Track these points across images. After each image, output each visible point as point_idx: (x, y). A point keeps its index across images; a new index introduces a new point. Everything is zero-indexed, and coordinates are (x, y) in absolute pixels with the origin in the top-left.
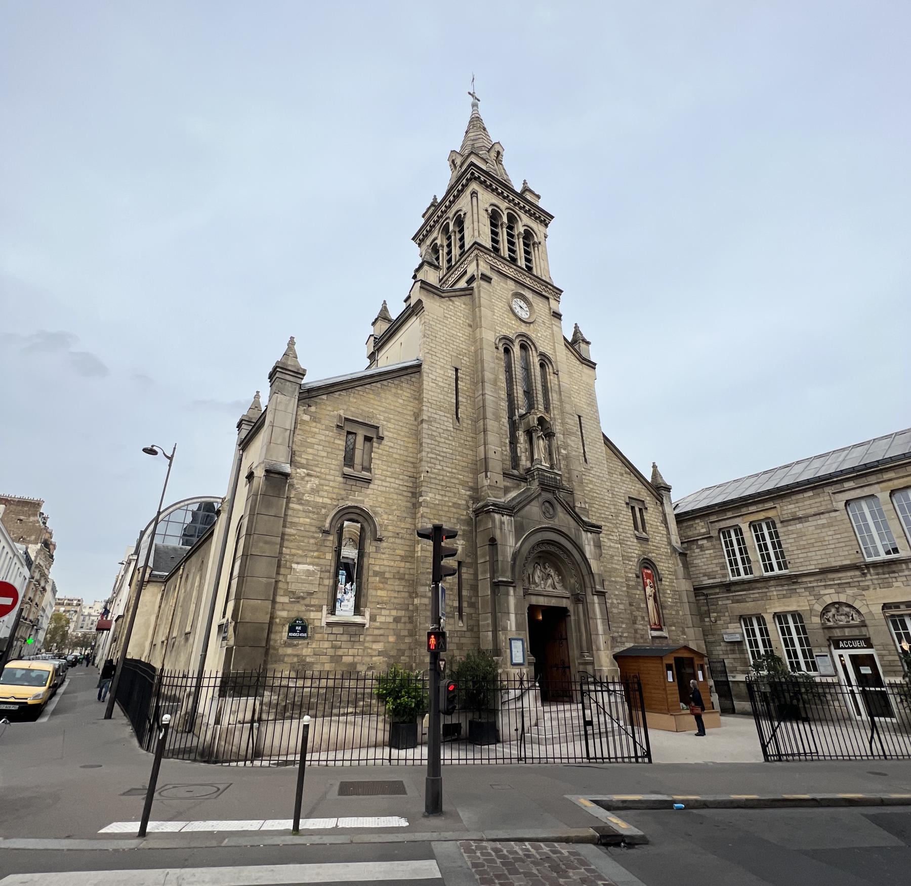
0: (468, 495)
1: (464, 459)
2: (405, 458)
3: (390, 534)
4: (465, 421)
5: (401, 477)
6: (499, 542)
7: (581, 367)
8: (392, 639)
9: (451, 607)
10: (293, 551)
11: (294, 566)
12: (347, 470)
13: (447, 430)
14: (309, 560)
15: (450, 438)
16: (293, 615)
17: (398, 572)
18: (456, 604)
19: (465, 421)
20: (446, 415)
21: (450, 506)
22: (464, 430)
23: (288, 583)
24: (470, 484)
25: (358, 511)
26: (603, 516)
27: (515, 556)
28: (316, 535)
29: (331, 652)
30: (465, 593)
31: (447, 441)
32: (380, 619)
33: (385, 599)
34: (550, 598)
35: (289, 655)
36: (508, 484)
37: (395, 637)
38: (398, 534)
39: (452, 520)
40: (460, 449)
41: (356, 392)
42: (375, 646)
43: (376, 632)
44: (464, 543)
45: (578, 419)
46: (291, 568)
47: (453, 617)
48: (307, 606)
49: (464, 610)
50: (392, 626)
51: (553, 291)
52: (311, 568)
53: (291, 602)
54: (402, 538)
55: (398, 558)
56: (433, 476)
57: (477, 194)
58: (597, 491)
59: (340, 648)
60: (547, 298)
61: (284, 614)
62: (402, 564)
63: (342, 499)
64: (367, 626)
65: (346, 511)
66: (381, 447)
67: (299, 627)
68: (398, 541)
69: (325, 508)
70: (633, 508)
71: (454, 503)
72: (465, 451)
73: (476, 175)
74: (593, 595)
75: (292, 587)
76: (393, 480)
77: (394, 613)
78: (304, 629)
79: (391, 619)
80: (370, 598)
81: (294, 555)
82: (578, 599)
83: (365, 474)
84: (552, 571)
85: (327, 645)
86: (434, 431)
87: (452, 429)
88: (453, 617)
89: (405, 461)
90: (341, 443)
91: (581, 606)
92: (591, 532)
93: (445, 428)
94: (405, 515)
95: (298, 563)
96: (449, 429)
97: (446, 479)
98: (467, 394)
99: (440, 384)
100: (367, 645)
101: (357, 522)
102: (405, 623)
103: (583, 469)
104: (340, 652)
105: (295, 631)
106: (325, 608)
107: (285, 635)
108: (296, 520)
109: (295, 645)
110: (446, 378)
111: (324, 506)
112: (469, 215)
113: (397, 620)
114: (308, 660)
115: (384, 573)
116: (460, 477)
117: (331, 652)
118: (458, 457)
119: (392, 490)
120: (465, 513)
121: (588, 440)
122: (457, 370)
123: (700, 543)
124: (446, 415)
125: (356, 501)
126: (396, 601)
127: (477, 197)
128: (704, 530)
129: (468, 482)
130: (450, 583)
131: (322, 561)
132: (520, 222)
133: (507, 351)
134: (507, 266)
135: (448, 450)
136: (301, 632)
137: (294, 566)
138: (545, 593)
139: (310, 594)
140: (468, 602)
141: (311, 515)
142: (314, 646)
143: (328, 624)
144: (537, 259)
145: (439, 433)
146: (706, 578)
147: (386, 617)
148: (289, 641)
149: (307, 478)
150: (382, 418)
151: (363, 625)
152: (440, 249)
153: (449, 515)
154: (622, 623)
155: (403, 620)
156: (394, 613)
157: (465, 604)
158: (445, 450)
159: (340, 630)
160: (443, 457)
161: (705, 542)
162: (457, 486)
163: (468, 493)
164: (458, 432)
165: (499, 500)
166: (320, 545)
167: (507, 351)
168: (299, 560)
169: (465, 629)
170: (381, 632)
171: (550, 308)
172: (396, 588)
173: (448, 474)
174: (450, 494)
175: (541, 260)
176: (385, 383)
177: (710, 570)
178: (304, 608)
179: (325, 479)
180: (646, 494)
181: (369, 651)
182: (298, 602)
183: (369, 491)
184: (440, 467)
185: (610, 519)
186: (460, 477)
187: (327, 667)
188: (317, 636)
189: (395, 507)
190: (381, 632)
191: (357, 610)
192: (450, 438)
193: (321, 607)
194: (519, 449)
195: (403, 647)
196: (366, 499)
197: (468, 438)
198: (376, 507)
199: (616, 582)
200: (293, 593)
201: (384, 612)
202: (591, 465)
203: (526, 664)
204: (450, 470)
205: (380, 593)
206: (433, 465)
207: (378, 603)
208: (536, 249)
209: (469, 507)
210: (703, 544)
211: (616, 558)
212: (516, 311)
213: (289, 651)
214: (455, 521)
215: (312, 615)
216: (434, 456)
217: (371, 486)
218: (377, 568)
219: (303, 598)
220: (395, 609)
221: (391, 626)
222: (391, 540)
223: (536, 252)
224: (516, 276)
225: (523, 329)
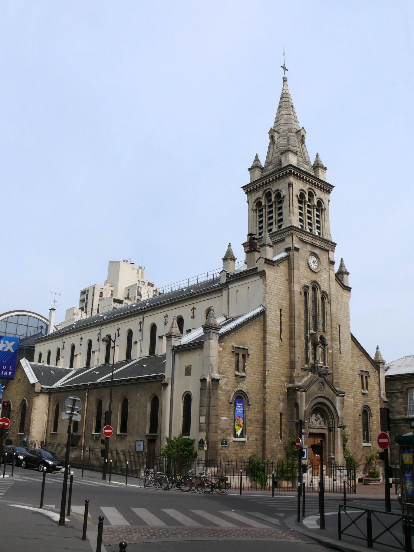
2: (258, 364)
5: (257, 373)
6: (299, 405)
7: (343, 292)
8: (255, 447)
9: (277, 434)
11: (221, 418)
12: (237, 373)
16: (222, 438)
17: (256, 419)
18: (279, 433)
25: (241, 392)
27: (305, 412)
28: (227, 404)
29: (235, 452)
30: (283, 427)
32: (251, 439)
36: (303, 374)
38: (256, 401)
43: (249, 444)
46: (220, 419)
47: (278, 438)
48: (226, 434)
50: (255, 442)
51: (332, 245)
52: (227, 418)
55: (256, 412)
56: (271, 372)
57: (292, 185)
58: (345, 370)
59: (238, 451)
60: (328, 251)
62: (258, 415)
64: (246, 442)
66: (249, 359)
67: (225, 442)
68: (256, 405)
69: (229, 392)
70: (362, 377)
71: (279, 385)
73: (293, 171)
74: (338, 428)
76: (253, 375)
77: (255, 436)
78: (226, 444)
79: (254, 439)
83: (243, 374)
85: (233, 449)
86: (271, 348)
87: (278, 346)
88: (278, 438)
89: (258, 365)
90: (234, 360)
92: (340, 396)
94: (259, 392)
95: (222, 417)
99: (274, 321)
100: (246, 449)
102: (259, 441)
104: (238, 452)
105: (223, 444)
106: (232, 435)
107: (220, 445)
109: (224, 449)
110: (276, 316)
111: (229, 391)
112: (287, 198)
113: (256, 439)
114: (228, 455)
115: (251, 420)
118: (281, 361)
121: (343, 340)
122: (281, 310)
123: (397, 394)
126: (256, 432)
127: (292, 187)
128: (399, 388)
131: (230, 416)
132: (315, 196)
133: (306, 294)
134: (308, 236)
137: (221, 418)
138: (316, 427)
139: (227, 429)
141: (225, 395)
143: (234, 441)
144: (323, 221)
145: (273, 349)
146: (396, 414)
147: (252, 438)
149: (223, 379)
150: (249, 343)
152: (264, 208)
155: (258, 440)
156: (255, 436)
157: (283, 433)
160: (275, 362)
161: (399, 394)
162: (281, 376)
165: (299, 383)
166: (229, 408)
167: (306, 294)
168: (223, 415)
170: (251, 444)
171: (329, 258)
175: (326, 222)
177: (400, 410)
179: (229, 378)
180: (370, 367)
181: (247, 452)
182: (224, 433)
183: (245, 382)
184: (273, 367)
185: (350, 385)
187: (234, 458)
188: (230, 446)
192: (278, 351)
193: (231, 434)
194: (309, 353)
195: (259, 450)
196: (244, 387)
199: (349, 419)
200: (222, 429)
201: (252, 436)
203: (308, 458)
204: (277, 368)
207: (250, 433)
208: (323, 213)
210: (398, 395)
212: (311, 265)
213: (222, 451)
216: (271, 362)
217: (246, 379)
219: (225, 431)
220: (256, 435)
222: (254, 404)
223: (323, 215)
224: (312, 241)
225: (314, 277)
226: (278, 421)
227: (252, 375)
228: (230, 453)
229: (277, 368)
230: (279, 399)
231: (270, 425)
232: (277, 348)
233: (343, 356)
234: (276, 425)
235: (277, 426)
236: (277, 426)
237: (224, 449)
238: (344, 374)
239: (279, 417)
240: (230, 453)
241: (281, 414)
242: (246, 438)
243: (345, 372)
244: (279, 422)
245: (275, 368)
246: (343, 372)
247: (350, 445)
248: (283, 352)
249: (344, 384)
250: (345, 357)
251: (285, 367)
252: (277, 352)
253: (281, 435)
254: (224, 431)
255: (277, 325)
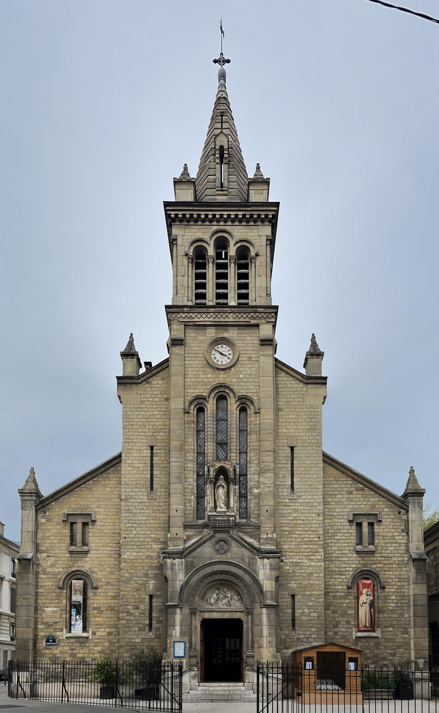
0: (160, 548)
1: (157, 521)
2: (113, 531)
3: (104, 584)
4: (159, 490)
5: (110, 545)
7: (305, 389)
10: (44, 601)
11: (45, 609)
12: (73, 548)
13: (142, 502)
14: (53, 605)
15: (145, 508)
16: (48, 634)
17: (110, 606)
18: (147, 622)
19: (159, 490)
20: (141, 490)
21: (144, 559)
22: (157, 498)
23: (43, 618)
24: (162, 540)
25: (81, 573)
26: (306, 539)
27: (182, 588)
28: (56, 591)
29: (70, 652)
30: (154, 615)
31: (142, 511)
32: (98, 634)
33: (101, 622)
34: (223, 613)
35: (47, 654)
37: (108, 643)
38: (109, 583)
39: (145, 568)
40: (153, 514)
41: (75, 493)
42: (96, 648)
43: (96, 641)
44: (155, 582)
45: (290, 451)
46: (44, 610)
47: (144, 630)
48: (54, 629)
49: (153, 625)
50: (108, 637)
52: (54, 609)
53: (46, 628)
54: (112, 585)
55: (109, 598)
58: (302, 518)
59: (75, 649)
61: (43, 634)
62: (113, 601)
63: (70, 567)
64: (90, 638)
65: (73, 574)
66: (95, 527)
68: (109, 587)
69: (59, 574)
71: (147, 556)
72: (158, 515)
75: (46, 620)
77: (108, 630)
78: (54, 641)
79: (105, 634)
80: (91, 623)
81: (44, 603)
82: (249, 612)
83: (85, 548)
84: (229, 593)
86: (130, 506)
87: (146, 500)
88: (144, 630)
89: (113, 533)
90: (67, 532)
91: (250, 617)
93: (140, 501)
94: (114, 570)
95: (47, 607)
96: (143, 500)
97: (141, 539)
98: (162, 466)
99: (137, 465)
100: (91, 648)
101: (81, 579)
102: (115, 635)
103: (288, 501)
104: (75, 652)
105: (49, 642)
106: (64, 630)
107: (44, 644)
108: (43, 584)
110: (141, 458)
111: (59, 573)
113: (109, 634)
114: (57, 655)
115: (100, 607)
116: (152, 536)
117: (70, 652)
118: (151, 521)
119: (104, 555)
120: (156, 561)
121: (300, 469)
122: (152, 448)
124: (141, 490)
125: (79, 567)
126: (108, 623)
129: (159, 538)
130: (142, 610)
131: (60, 605)
135: (143, 518)
136: (52, 642)
137: (45, 609)
139: (56, 623)
140: (156, 620)
141: (52, 580)
142: (60, 649)
143: (67, 638)
145: (135, 506)
147: (102, 632)
148: (46, 647)
149: (47, 559)
150: (94, 506)
151: (88, 638)
153: (142, 565)
154: (312, 627)
155: (113, 634)
156: (108, 630)
157: (154, 622)
158: (139, 518)
159: (74, 640)
160: (138, 524)
162: (150, 543)
163: (159, 546)
164: (152, 501)
166: (59, 596)
168: (48, 605)
169: (153, 637)
170: (100, 641)
172: (109, 616)
173: (142, 536)
174: (144, 550)
176: (96, 479)
178: (53, 630)
179: (58, 557)
180: (383, 506)
181: (92, 651)
182: (49, 627)
183: (87, 559)
184: (135, 532)
185: (316, 541)
186: (152, 536)
189: (106, 566)
190: (100, 641)
191: (85, 629)
192: (145, 508)
195: (113, 648)
197: (161, 504)
198: (93, 568)
199: (311, 595)
200: (46, 623)
201: (100, 630)
202: (299, 494)
204: (144, 532)
205: (97, 619)
206: (130, 532)
207: (97, 625)
209: (160, 557)
211: (315, 575)
213: (47, 651)
214: (148, 568)
215: (58, 634)
216: (130, 525)
217: (89, 555)
218: (95, 605)
219: (52, 625)
220: (108, 627)
221: (106, 637)
222: (104, 587)
226: (145, 607)
227: (100, 548)
228: (61, 653)
229: (142, 532)
230: (146, 575)
231: (128, 612)
232: (144, 504)
233: (300, 496)
234: (141, 611)
235: (144, 614)
236: (144, 614)
237: (51, 649)
238: (300, 524)
239: (147, 600)
240: (61, 653)
241: (151, 597)
242: (90, 633)
243: (303, 520)
244: (148, 608)
245: (138, 534)
246: (299, 522)
247: (313, 636)
248: (156, 508)
249: (300, 540)
250: (303, 497)
251: (159, 529)
252: (143, 509)
253: (150, 625)
254: (49, 625)
255: (143, 471)
